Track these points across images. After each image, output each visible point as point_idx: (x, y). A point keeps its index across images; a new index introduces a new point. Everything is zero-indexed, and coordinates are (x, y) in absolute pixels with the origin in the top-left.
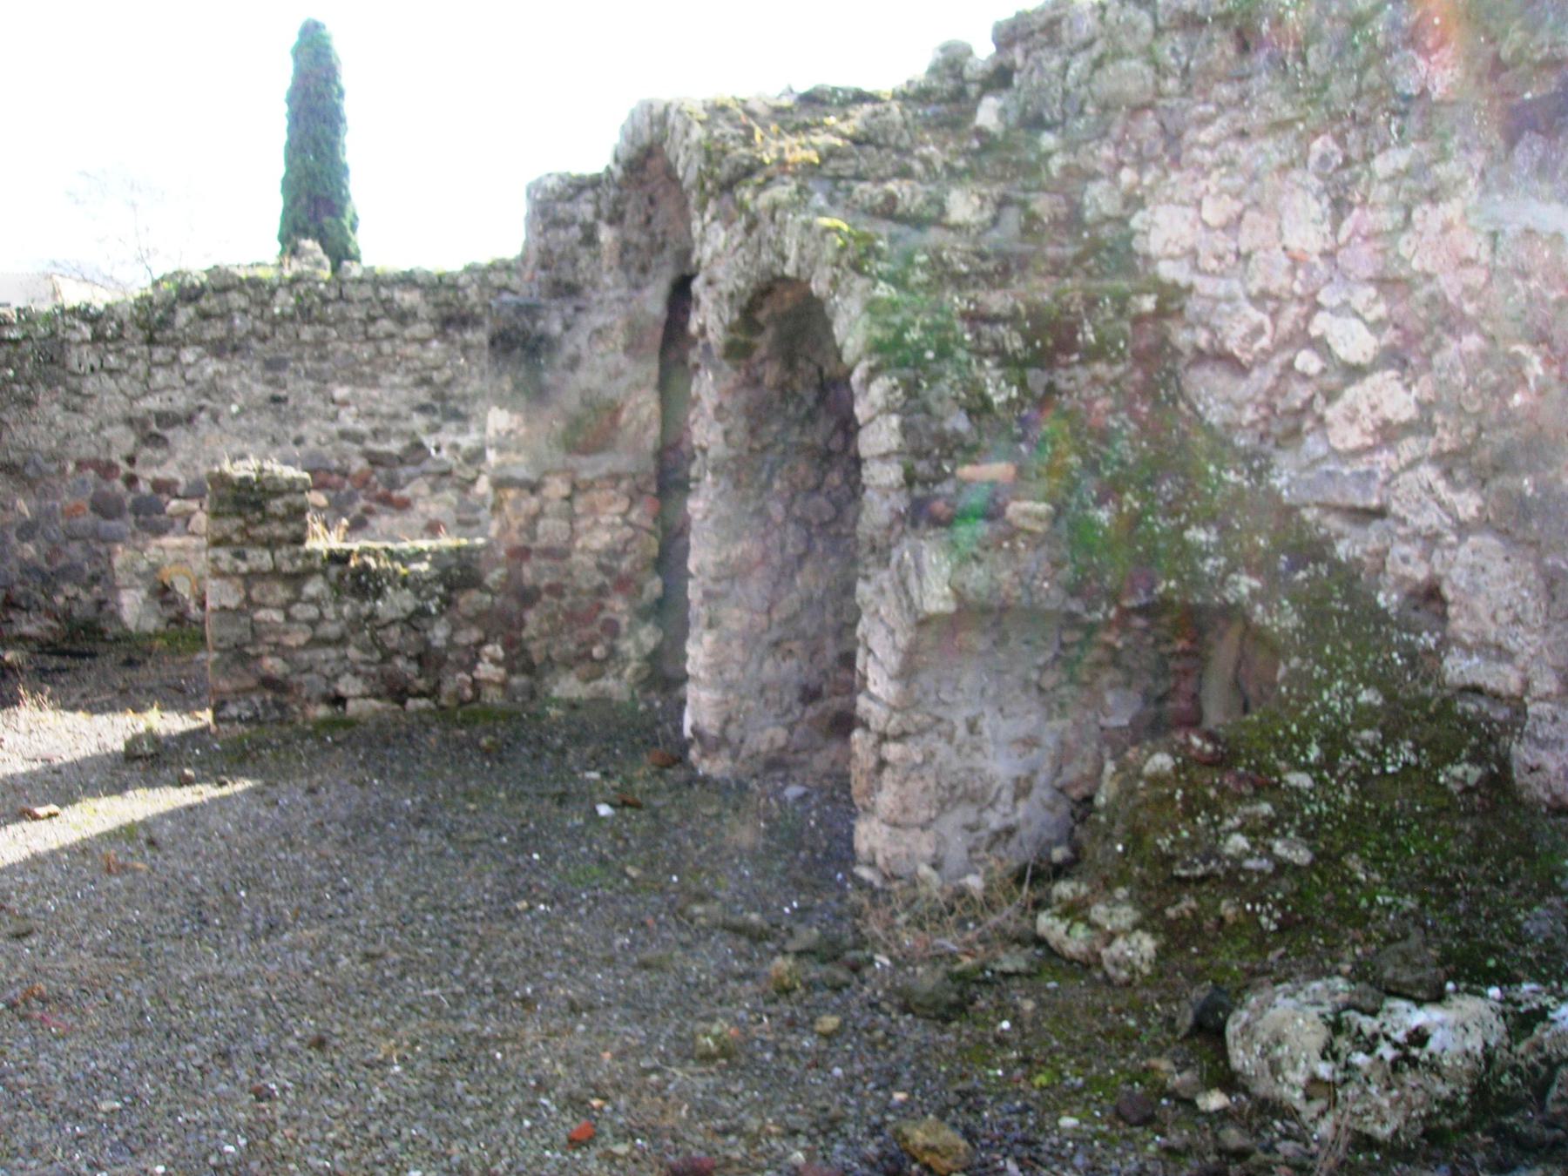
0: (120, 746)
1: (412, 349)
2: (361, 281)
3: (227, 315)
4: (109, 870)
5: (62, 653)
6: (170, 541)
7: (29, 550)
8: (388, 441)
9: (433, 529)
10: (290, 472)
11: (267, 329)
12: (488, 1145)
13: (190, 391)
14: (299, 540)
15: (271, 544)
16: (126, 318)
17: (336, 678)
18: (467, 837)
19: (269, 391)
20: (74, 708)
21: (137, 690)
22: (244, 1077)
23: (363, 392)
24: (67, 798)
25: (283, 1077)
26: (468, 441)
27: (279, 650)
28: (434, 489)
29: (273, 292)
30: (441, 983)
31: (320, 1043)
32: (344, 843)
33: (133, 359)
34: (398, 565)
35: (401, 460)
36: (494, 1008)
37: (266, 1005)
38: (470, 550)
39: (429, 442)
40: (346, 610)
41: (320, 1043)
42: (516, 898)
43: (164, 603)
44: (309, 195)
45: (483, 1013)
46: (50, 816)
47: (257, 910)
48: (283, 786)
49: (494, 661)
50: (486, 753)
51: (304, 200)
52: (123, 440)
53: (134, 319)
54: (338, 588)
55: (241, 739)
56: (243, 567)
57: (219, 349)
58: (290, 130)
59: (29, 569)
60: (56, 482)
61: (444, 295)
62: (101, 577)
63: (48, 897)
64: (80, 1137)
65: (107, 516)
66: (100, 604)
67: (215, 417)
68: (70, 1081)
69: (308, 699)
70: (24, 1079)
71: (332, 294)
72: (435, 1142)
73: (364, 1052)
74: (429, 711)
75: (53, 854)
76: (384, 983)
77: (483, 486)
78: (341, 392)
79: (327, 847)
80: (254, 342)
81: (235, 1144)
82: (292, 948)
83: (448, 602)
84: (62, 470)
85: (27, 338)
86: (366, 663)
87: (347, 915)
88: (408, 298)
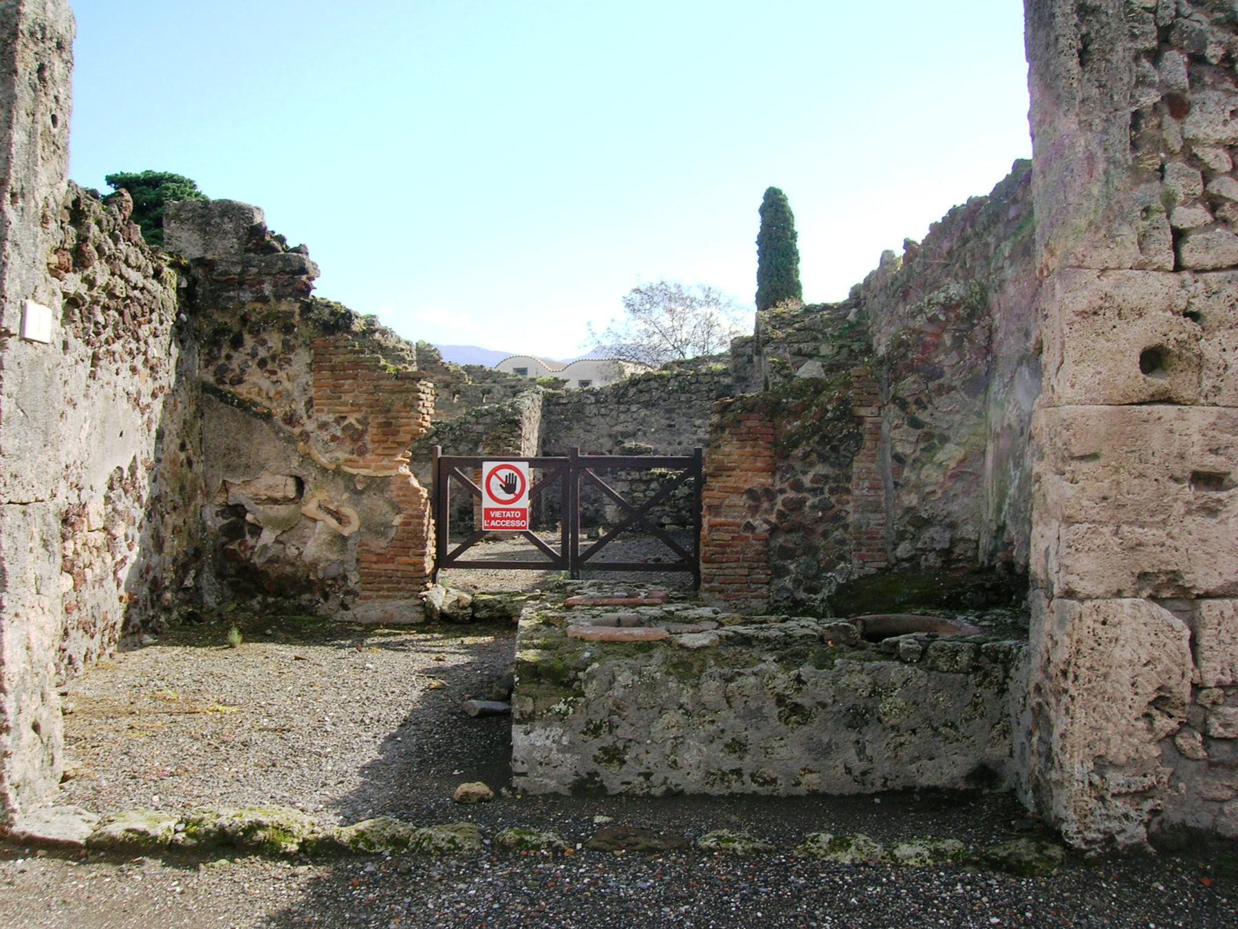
2: (706, 374)
19: (668, 422)
29: (669, 381)
53: (611, 394)
57: (647, 405)
66: (597, 511)
67: (645, 434)
78: (698, 422)
80: (661, 402)
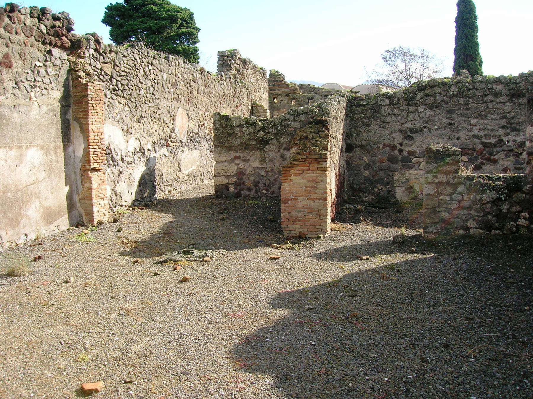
0: (391, 238)
1: (499, 106)
2: (481, 82)
3: (434, 95)
4: (383, 279)
5: (376, 207)
6: (412, 172)
7: (367, 173)
8: (490, 139)
9: (505, 170)
10: (454, 148)
11: (448, 100)
12: (502, 393)
13: (421, 121)
14: (456, 172)
15: (447, 173)
16: (400, 97)
17: (467, 220)
18: (509, 281)
19: (449, 121)
20: (378, 225)
21: (399, 221)
22: (419, 354)
23: (481, 121)
24: (373, 254)
25: (432, 356)
26: (519, 139)
27: (447, 210)
28: (506, 156)
29: (450, 87)
30: (493, 332)
31: (447, 346)
32: (464, 278)
33: (402, 110)
34: (491, 182)
35: (495, 146)
36: (511, 344)
37: (430, 330)
38: (518, 178)
39: (505, 139)
40: (472, 197)
41: (447, 346)
42: (525, 305)
43: (410, 192)
44: (464, 54)
45: (507, 345)
46: (367, 259)
47: (431, 298)
48: (446, 257)
49: (525, 218)
50: (519, 252)
51: (463, 56)
52: (399, 137)
53: (403, 97)
54: (469, 189)
55: (432, 239)
56: (437, 181)
57: (431, 107)
58: (456, 32)
59: (366, 179)
60: (376, 151)
61: (511, 86)
62: (390, 183)
63: (363, 285)
64: (362, 364)
65: (393, 163)
66: (389, 192)
67: (429, 130)
68: (362, 345)
69: (456, 227)
70: (347, 342)
71: (471, 87)
72: (483, 387)
73: (462, 352)
74: (498, 234)
75: (366, 271)
76: (472, 329)
77: (524, 156)
78: (474, 121)
79: (458, 279)
80: (443, 104)
81: (412, 375)
82: (442, 312)
83: (509, 196)
84: (378, 147)
85: (368, 104)
86: (477, 216)
87: (462, 304)
88: (499, 88)
